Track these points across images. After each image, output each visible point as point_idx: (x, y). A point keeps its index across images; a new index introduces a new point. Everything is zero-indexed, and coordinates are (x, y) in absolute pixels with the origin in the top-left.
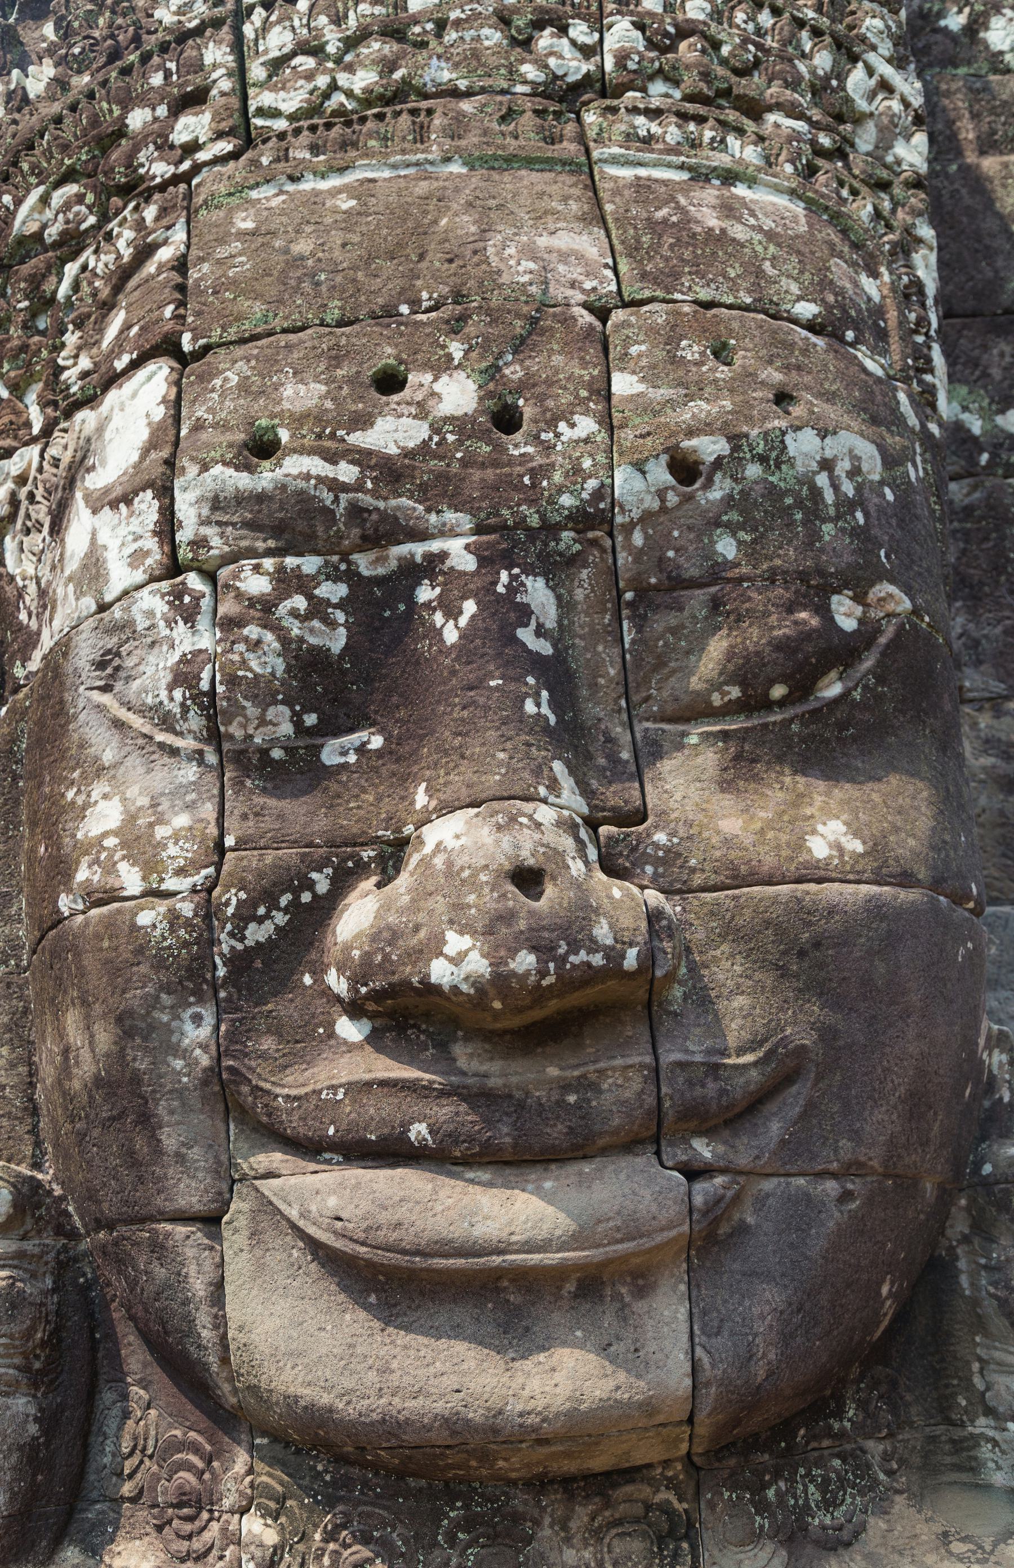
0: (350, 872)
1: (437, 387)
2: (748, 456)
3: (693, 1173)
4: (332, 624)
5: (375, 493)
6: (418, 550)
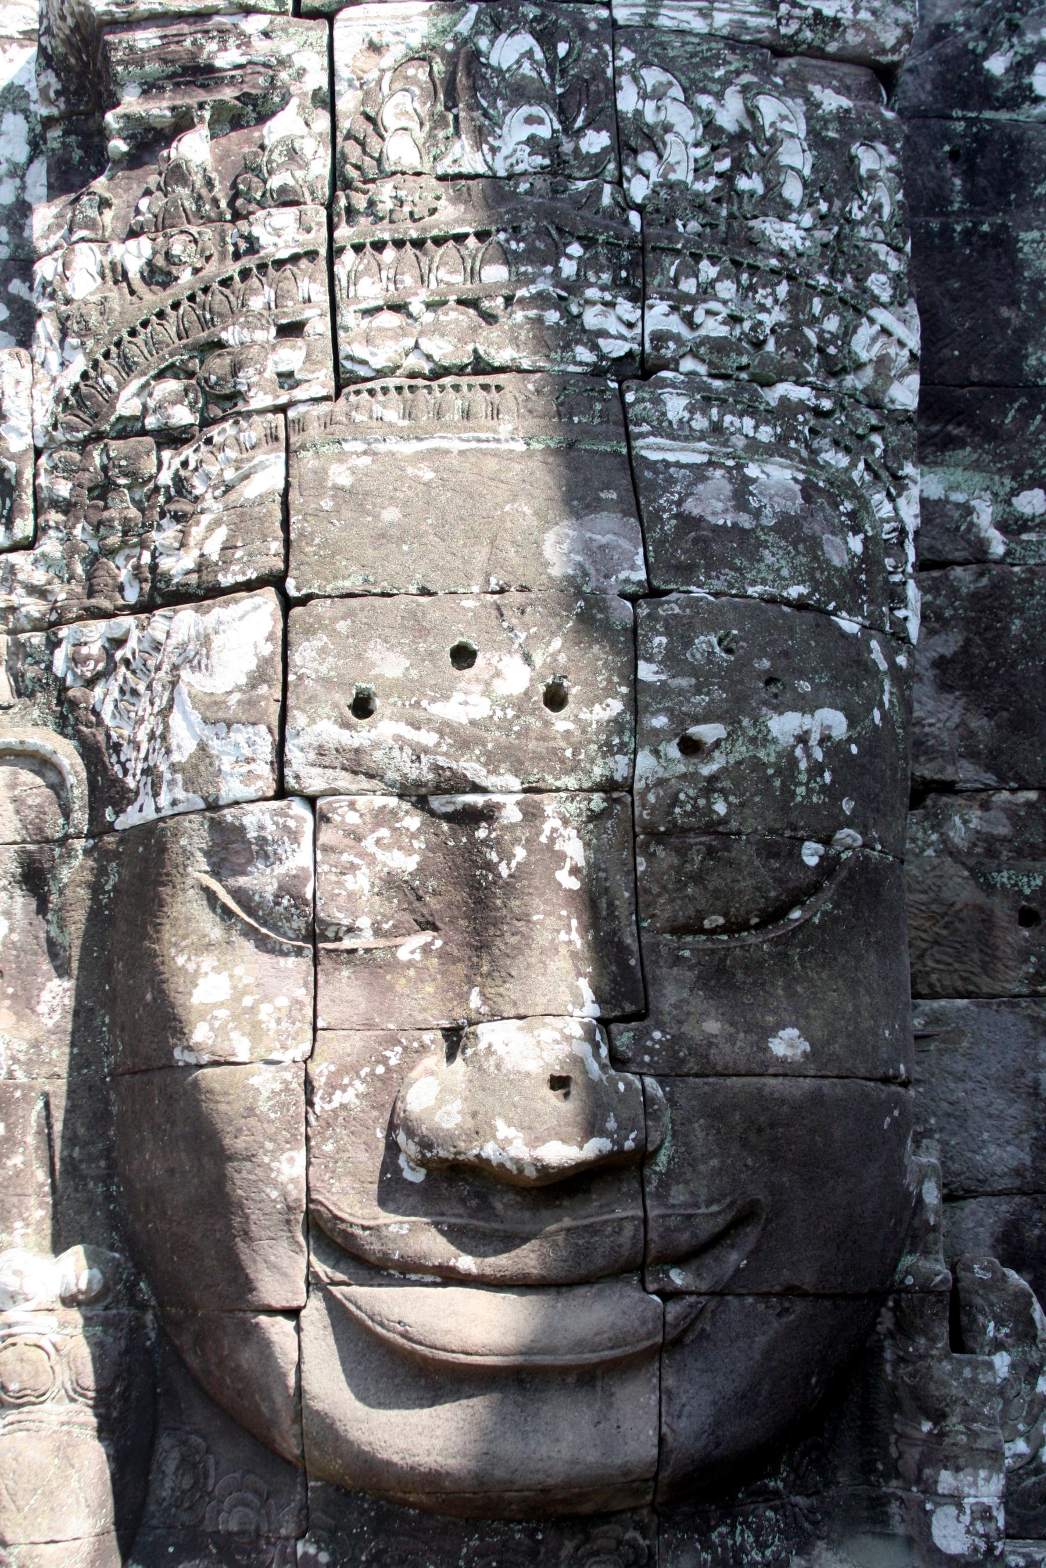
3: (668, 1295)
4: (410, 851)
6: (477, 800)
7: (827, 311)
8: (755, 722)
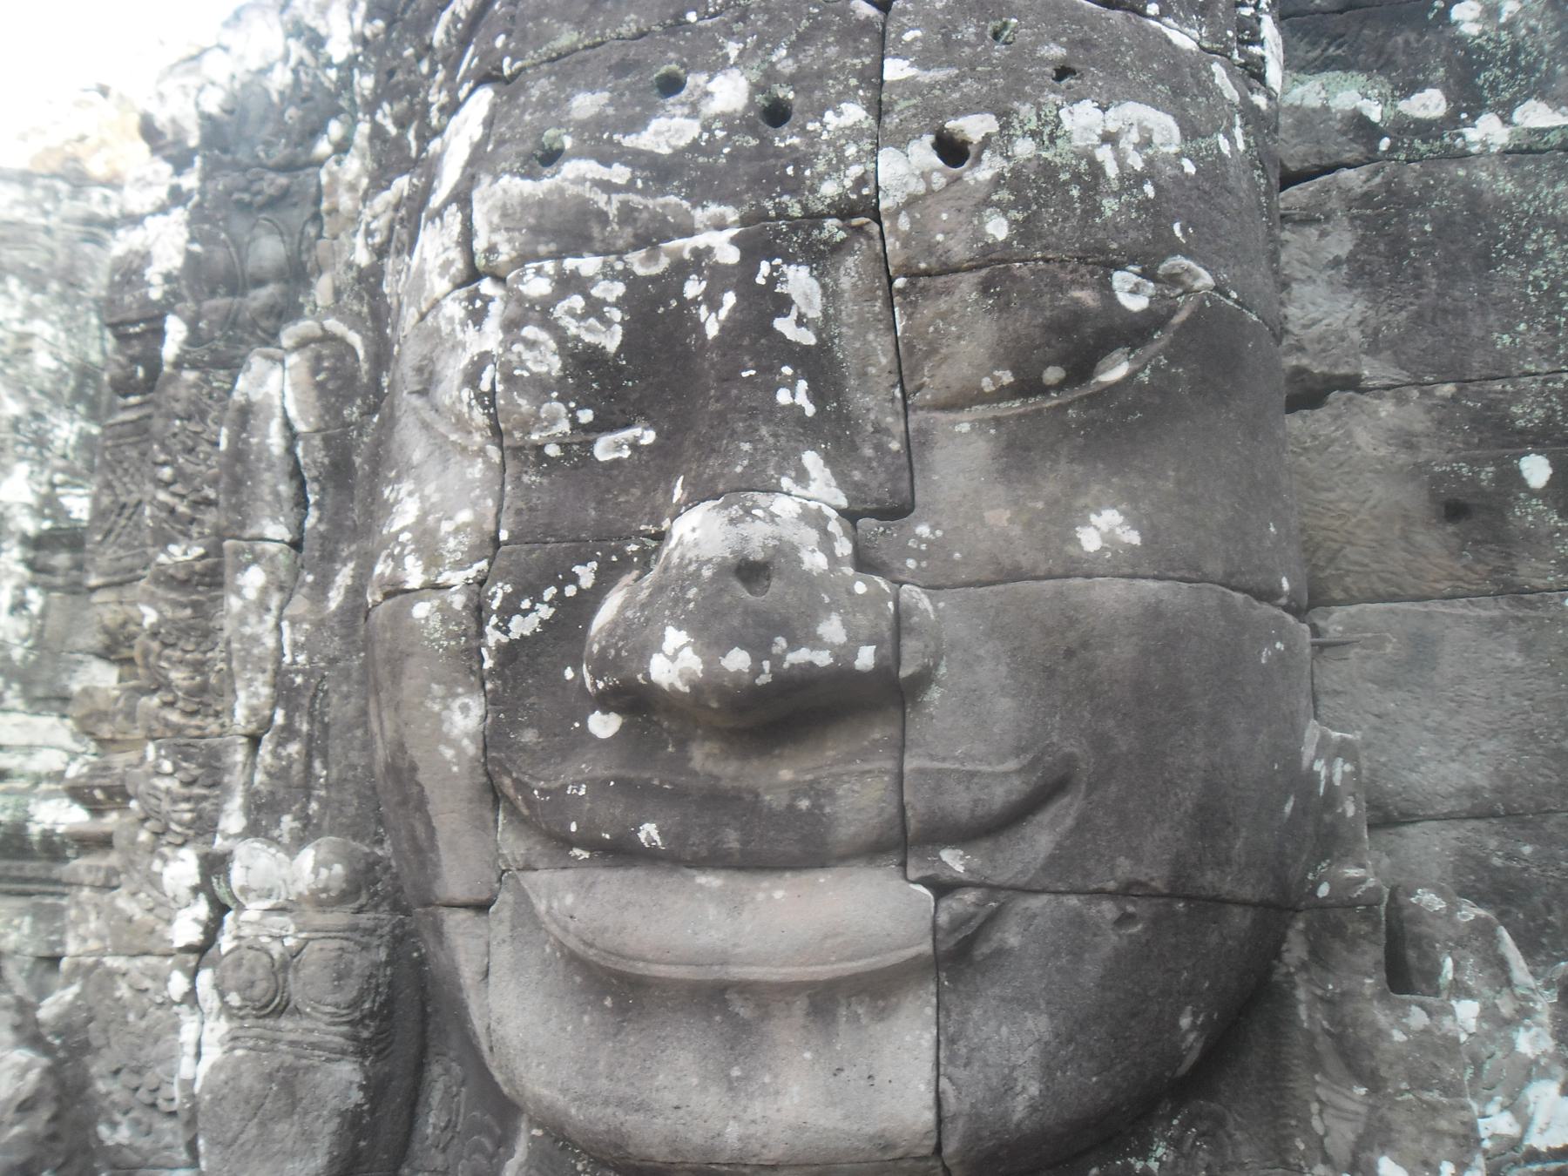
0: (613, 565)
1: (711, 87)
2: (1019, 133)
4: (608, 323)
5: (643, 193)
6: (684, 245)
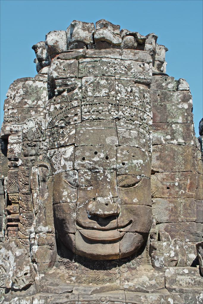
4: (89, 176)
6: (97, 170)
7: (141, 113)
8: (131, 161)
